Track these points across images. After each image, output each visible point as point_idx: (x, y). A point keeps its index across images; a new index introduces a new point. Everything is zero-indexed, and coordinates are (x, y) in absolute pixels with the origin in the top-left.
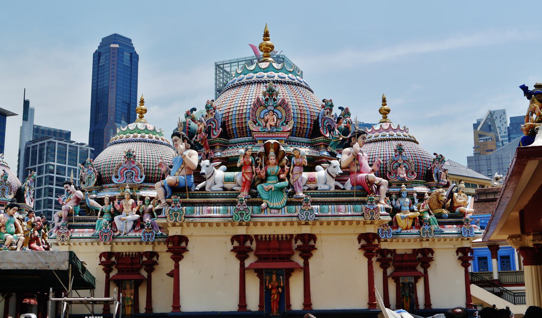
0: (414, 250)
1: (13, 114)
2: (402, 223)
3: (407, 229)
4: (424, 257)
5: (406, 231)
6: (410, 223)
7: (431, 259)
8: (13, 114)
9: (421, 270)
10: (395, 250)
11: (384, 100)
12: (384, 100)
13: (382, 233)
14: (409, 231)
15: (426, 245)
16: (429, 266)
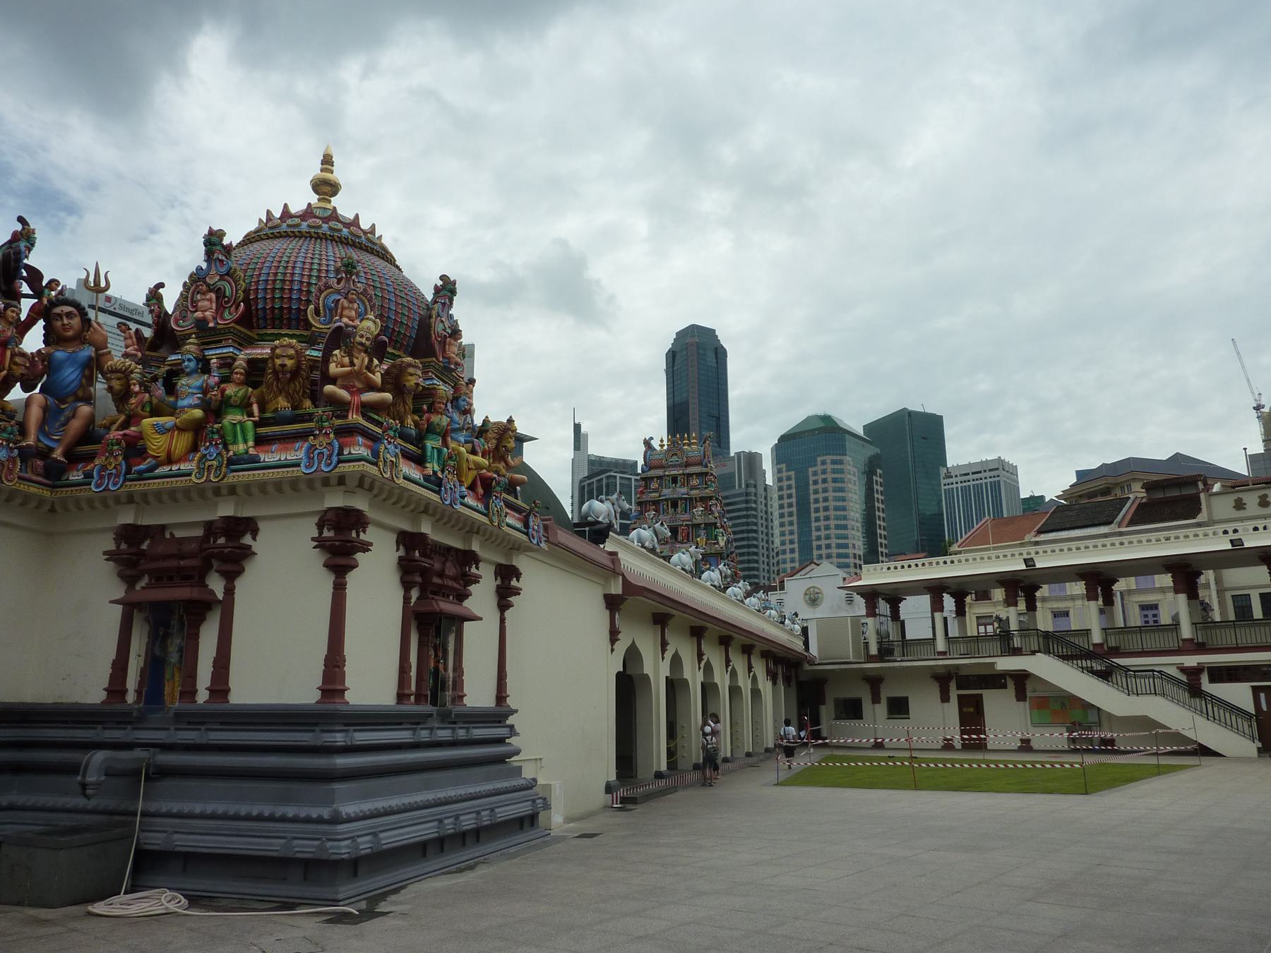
0: (209, 526)
1: (532, 439)
2: (157, 445)
3: (170, 460)
4: (229, 547)
5: (167, 468)
6: (181, 443)
7: (247, 553)
8: (532, 439)
9: (216, 585)
10: (163, 528)
11: (327, 161)
12: (327, 161)
13: (102, 477)
14: (175, 468)
15: (226, 509)
16: (239, 572)
